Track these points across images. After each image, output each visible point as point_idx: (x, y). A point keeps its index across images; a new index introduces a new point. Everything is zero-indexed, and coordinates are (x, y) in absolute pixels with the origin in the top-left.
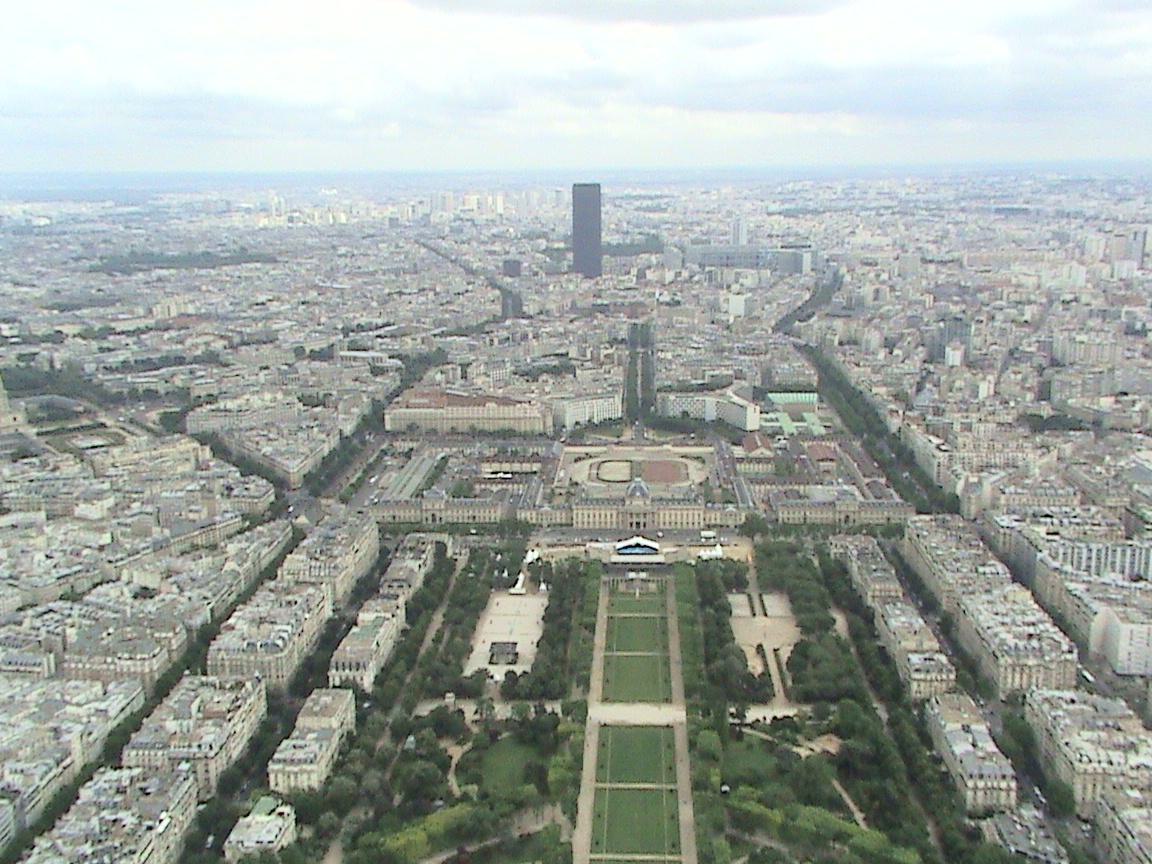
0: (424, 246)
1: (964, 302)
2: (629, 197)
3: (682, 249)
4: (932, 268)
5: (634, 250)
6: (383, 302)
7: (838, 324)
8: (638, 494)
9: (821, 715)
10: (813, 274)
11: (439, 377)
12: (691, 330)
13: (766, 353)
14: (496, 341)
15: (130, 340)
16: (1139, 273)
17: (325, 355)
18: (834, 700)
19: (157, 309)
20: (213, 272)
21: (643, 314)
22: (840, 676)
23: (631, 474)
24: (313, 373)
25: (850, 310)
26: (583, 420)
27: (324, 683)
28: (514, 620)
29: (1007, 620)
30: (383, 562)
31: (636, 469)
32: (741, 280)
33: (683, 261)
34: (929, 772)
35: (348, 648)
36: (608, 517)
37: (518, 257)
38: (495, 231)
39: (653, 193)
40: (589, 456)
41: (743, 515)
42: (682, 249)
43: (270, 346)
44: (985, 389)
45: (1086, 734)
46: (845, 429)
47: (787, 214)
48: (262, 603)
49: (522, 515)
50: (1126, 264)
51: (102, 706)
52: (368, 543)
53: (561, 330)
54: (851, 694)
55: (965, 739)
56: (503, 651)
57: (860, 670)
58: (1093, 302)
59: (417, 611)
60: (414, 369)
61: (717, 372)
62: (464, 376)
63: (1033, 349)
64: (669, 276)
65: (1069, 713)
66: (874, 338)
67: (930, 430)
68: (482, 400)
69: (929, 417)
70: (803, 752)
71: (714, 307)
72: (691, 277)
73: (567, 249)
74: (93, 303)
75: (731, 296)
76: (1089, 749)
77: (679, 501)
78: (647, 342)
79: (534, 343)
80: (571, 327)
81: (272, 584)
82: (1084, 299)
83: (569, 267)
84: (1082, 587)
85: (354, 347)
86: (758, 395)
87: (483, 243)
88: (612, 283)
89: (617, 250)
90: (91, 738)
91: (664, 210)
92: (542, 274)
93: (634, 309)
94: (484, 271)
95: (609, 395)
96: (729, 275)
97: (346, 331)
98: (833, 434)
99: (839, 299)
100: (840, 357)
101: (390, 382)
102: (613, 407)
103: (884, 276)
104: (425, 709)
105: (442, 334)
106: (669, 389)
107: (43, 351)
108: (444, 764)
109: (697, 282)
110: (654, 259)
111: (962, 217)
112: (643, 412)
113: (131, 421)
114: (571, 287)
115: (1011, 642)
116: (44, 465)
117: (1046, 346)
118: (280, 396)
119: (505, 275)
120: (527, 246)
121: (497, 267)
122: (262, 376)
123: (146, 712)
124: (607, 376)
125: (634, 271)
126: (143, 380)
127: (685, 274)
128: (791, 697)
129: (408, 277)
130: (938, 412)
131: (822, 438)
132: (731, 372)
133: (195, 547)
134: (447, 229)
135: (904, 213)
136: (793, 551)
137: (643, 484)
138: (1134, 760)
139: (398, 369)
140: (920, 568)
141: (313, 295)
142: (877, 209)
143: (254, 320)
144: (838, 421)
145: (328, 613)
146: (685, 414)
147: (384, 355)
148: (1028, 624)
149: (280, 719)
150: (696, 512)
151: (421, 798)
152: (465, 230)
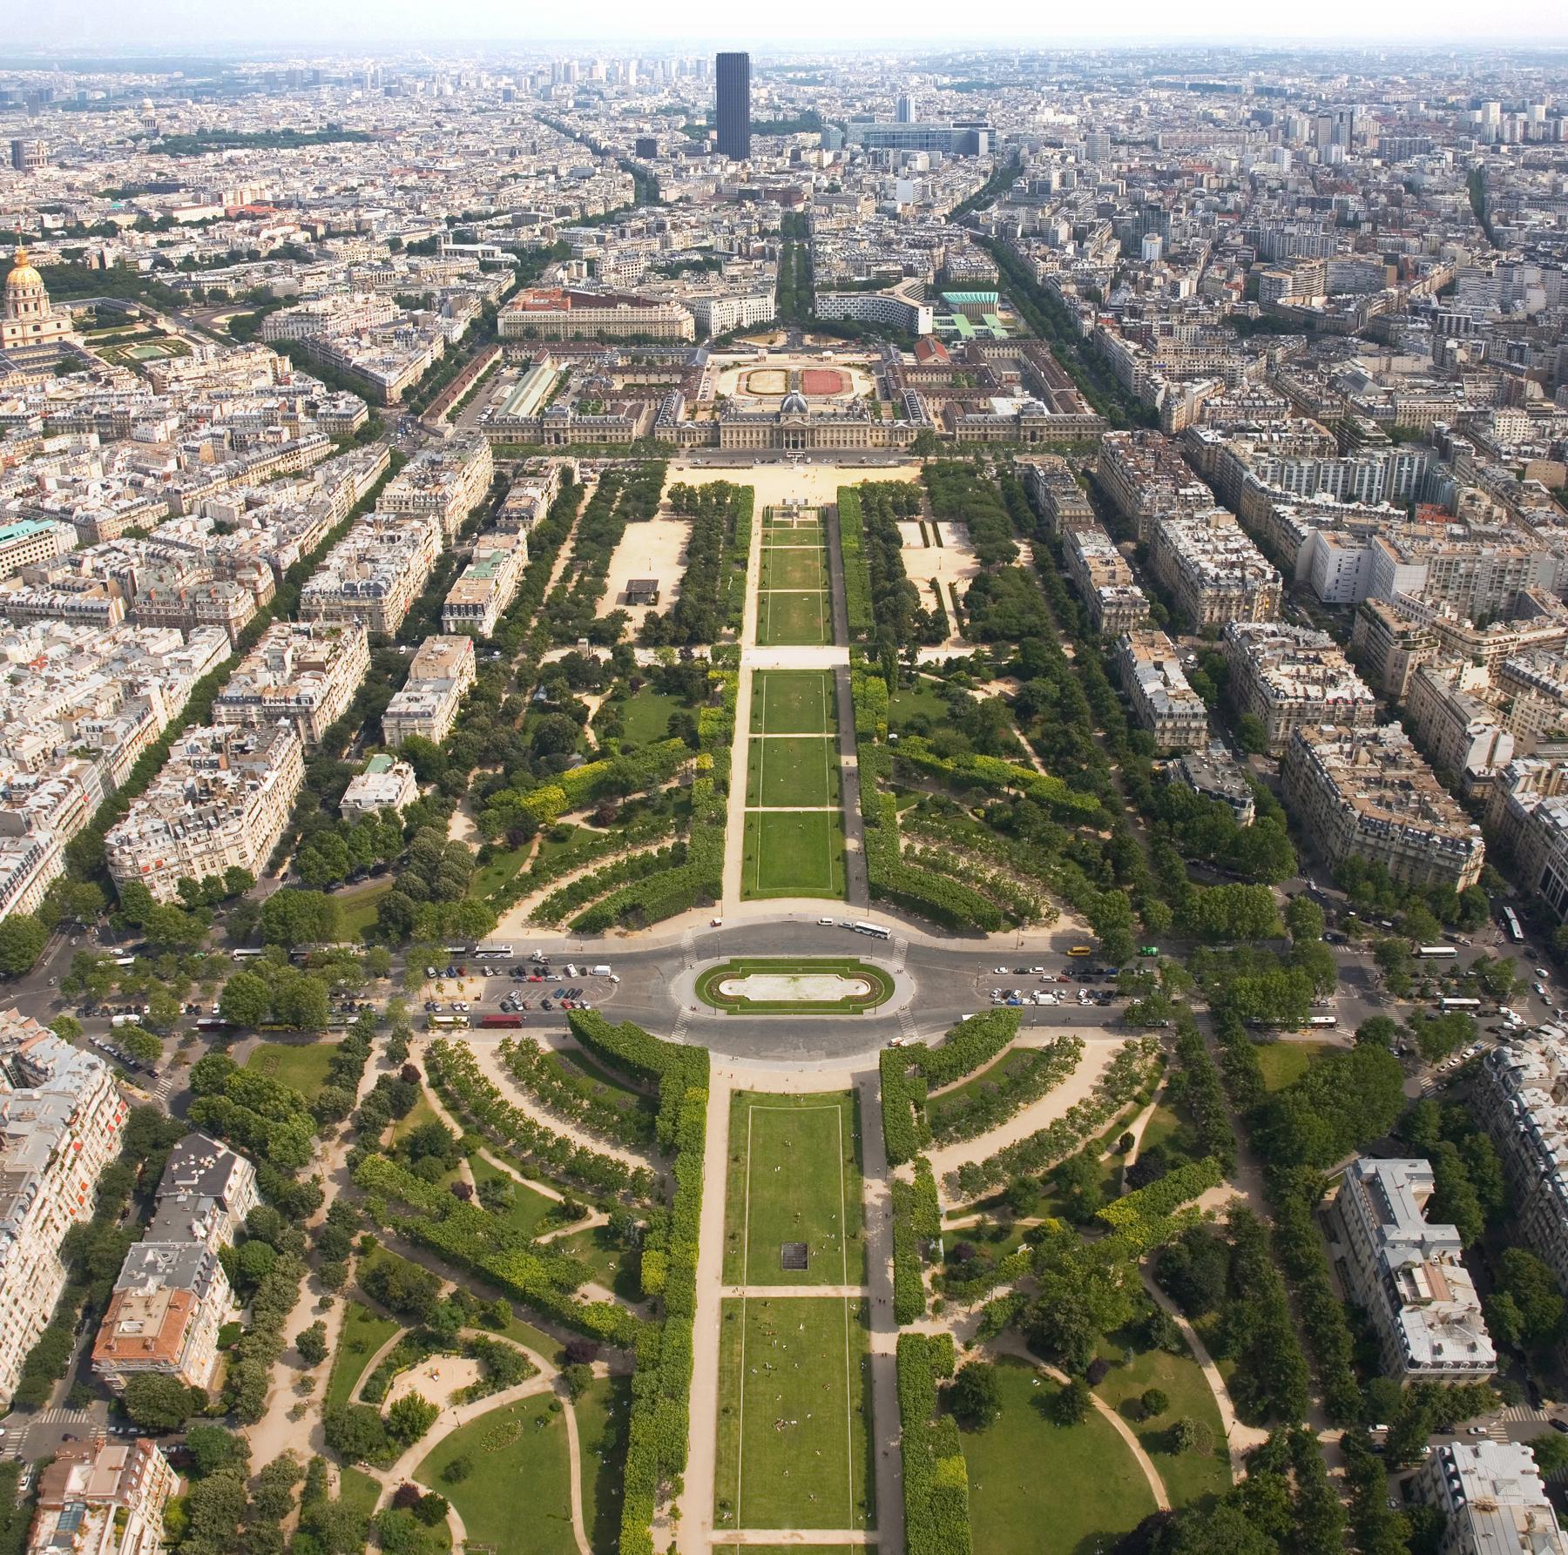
0: (545, 122)
1: (1161, 188)
3: (842, 126)
4: (1123, 151)
5: (787, 128)
7: (1021, 212)
9: (998, 654)
11: (561, 274)
15: (195, 233)
16: (1347, 158)
17: (428, 248)
18: (1014, 639)
19: (228, 198)
20: (295, 152)
21: (800, 200)
22: (1022, 613)
26: (731, 325)
27: (439, 628)
28: (651, 553)
29: (1209, 547)
30: (500, 487)
31: (792, 380)
34: (1115, 713)
35: (461, 592)
37: (653, 136)
40: (737, 364)
43: (362, 239)
44: (1187, 288)
45: (1285, 669)
47: (960, 88)
48: (361, 538)
50: (1334, 149)
51: (184, 656)
52: (482, 467)
54: (1033, 632)
55: (1163, 676)
56: (639, 592)
57: (1044, 606)
59: (543, 547)
60: (531, 264)
64: (828, 158)
65: (1272, 647)
66: (1063, 231)
67: (1127, 334)
68: (610, 301)
70: (979, 696)
71: (881, 193)
73: (710, 128)
74: (154, 188)
76: (1287, 685)
80: (716, 216)
81: (369, 517)
82: (1291, 186)
84: (1290, 510)
85: (460, 238)
86: (932, 294)
87: (613, 119)
88: (763, 162)
89: (766, 129)
90: (174, 693)
91: (821, 84)
93: (789, 196)
94: (615, 151)
95: (759, 291)
97: (451, 221)
98: (1016, 340)
100: (1023, 250)
102: (764, 307)
103: (1071, 159)
104: (554, 656)
105: (565, 225)
106: (828, 287)
107: (92, 245)
108: (580, 715)
111: (1153, 94)
112: (798, 315)
113: (197, 328)
114: (717, 170)
115: (1212, 571)
116: (95, 377)
117: (1251, 238)
118: (372, 296)
123: (233, 663)
125: (788, 152)
126: (208, 280)
127: (846, 156)
128: (967, 637)
130: (1135, 313)
133: (278, 476)
134: (571, 104)
135: (1090, 89)
136: (971, 472)
137: (801, 398)
138: (1332, 694)
139: (512, 265)
140: (1116, 489)
141: (411, 180)
142: (1060, 84)
145: (437, 548)
147: (497, 250)
148: (1232, 551)
149: (388, 671)
151: (550, 751)
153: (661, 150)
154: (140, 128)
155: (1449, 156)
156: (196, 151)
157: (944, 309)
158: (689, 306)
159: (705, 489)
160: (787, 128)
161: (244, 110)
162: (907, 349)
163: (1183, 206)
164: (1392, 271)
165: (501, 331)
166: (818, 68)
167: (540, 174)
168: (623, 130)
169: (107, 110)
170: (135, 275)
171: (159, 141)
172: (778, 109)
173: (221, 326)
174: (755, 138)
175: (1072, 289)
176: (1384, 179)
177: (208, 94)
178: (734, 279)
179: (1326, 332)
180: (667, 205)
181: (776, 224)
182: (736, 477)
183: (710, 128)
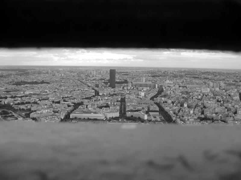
0: (80, 81)
2: (121, 72)
5: (122, 83)
6: (70, 92)
7: (163, 99)
10: (158, 88)
11: (82, 107)
14: (93, 100)
17: (59, 102)
21: (124, 96)
24: (56, 106)
25: (165, 96)
32: (143, 89)
38: (94, 78)
39: (125, 71)
44: (192, 112)
46: (165, 120)
47: (153, 76)
53: (107, 98)
58: (211, 95)
61: (139, 108)
62: (87, 107)
63: (200, 104)
66: (170, 101)
69: (181, 117)
71: (138, 95)
72: (133, 89)
75: (142, 93)
78: (124, 101)
79: (101, 101)
85: (64, 101)
86: (147, 113)
91: (128, 75)
92: (103, 87)
96: (140, 88)
97: (63, 98)
99: (163, 94)
101: (71, 108)
102: (117, 114)
103: (172, 89)
106: (129, 111)
109: (135, 90)
111: (186, 78)
113: (19, 115)
114: (109, 90)
118: (49, 111)
119: (96, 87)
120: (100, 81)
121: (94, 86)
122: (46, 107)
125: (122, 87)
126: (22, 107)
127: (132, 88)
129: (76, 87)
131: (160, 121)
132: (141, 108)
134: (84, 78)
143: (44, 95)
144: (163, 118)
146: (132, 116)
152: (88, 78)
153: (100, 86)
154: (11, 81)
155: (236, 90)
156: (20, 85)
157: (149, 116)
158: (104, 114)
160: (122, 83)
161: (28, 78)
163: (191, 98)
164: (226, 110)
165: (71, 117)
166: (128, 72)
167: (78, 90)
168: (93, 83)
169: (6, 77)
170: (10, 106)
171: (14, 83)
172: (121, 79)
173: (23, 115)
175: (172, 112)
176: (225, 94)
177: (23, 75)
179: (215, 120)
180: (101, 96)
181: (119, 100)
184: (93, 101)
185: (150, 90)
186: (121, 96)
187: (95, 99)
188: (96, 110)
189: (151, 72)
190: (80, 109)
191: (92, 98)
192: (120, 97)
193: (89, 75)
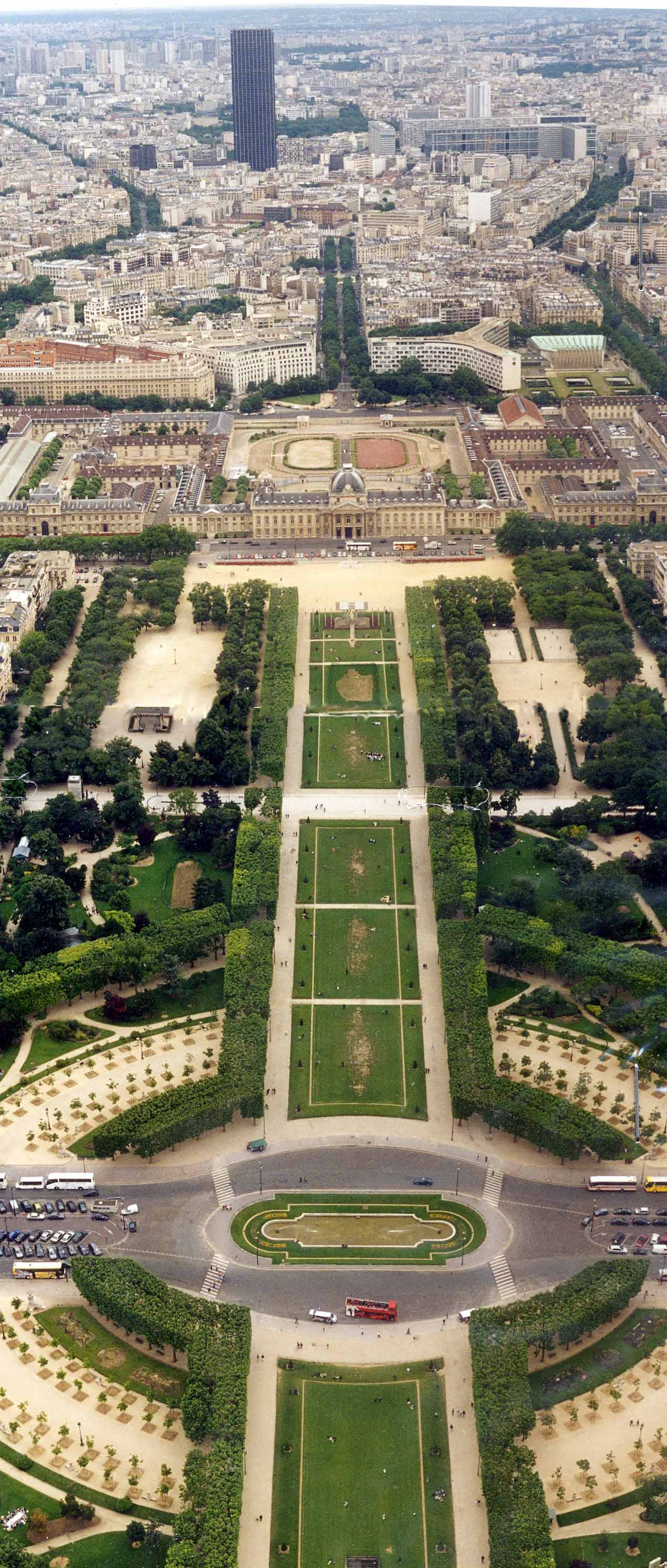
7: (629, 232)
8: (348, 487)
10: (589, 159)
12: (413, 244)
13: (526, 276)
23: (335, 458)
31: (344, 451)
32: (484, 170)
33: (398, 145)
36: (303, 521)
37: (151, 140)
38: (113, 100)
41: (503, 516)
42: (396, 125)
46: (645, 387)
49: (176, 522)
62: (80, 318)
64: (377, 164)
71: (445, 210)
72: (410, 167)
77: (409, 496)
78: (349, 264)
83: (229, 154)
86: (517, 337)
87: (100, 119)
92: (188, 165)
93: (328, 215)
96: (466, 162)
102: (306, 361)
105: (44, 257)
110: (353, 139)
120: (162, 121)
124: (292, 314)
125: (325, 158)
127: (401, 162)
134: (42, 100)
150: (434, 512)
152: (70, 99)
159: (236, 592)
160: (326, 127)
162: (490, 409)
168: (111, 134)
172: (312, 102)
174: (282, 138)
178: (262, 324)
180: (174, 229)
181: (313, 252)
182: (274, 576)
183: (226, 128)
184: (118, 267)
185: (534, 175)
186: (323, 226)
187: (138, 255)
188: (147, 333)
189: (533, 36)
190: (32, 329)
191: (109, 247)
192: (315, 235)
193: (77, 77)
